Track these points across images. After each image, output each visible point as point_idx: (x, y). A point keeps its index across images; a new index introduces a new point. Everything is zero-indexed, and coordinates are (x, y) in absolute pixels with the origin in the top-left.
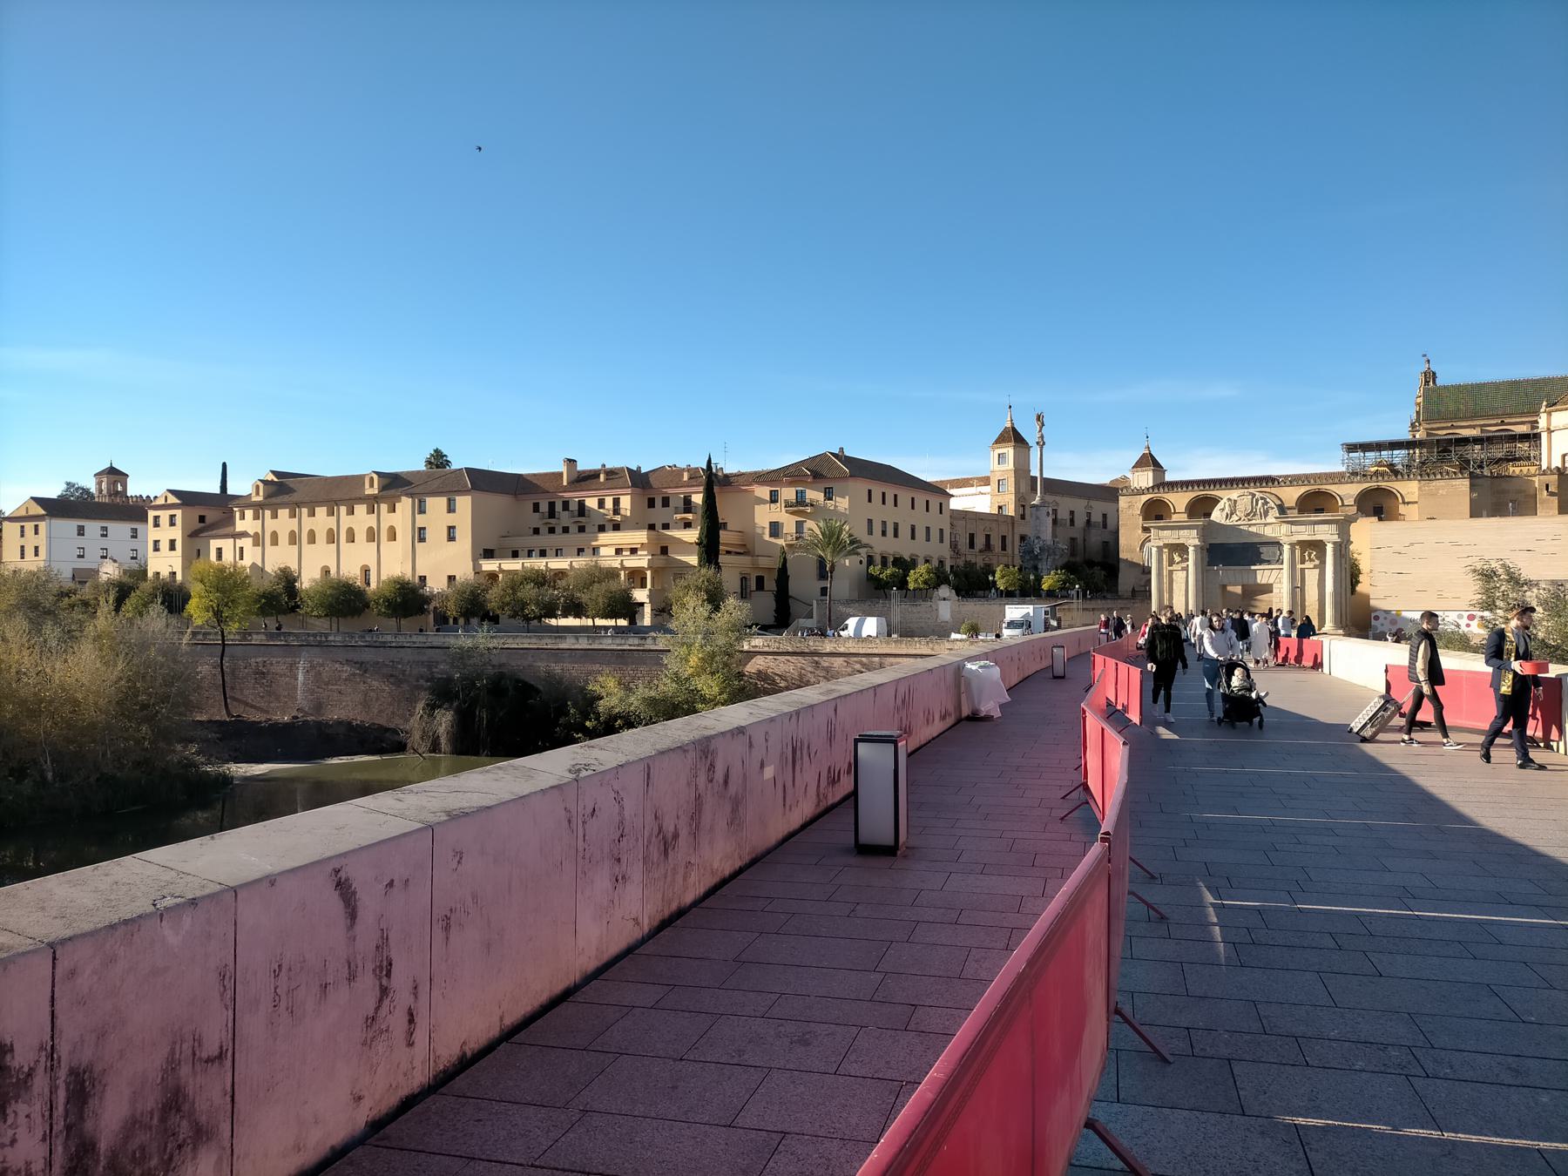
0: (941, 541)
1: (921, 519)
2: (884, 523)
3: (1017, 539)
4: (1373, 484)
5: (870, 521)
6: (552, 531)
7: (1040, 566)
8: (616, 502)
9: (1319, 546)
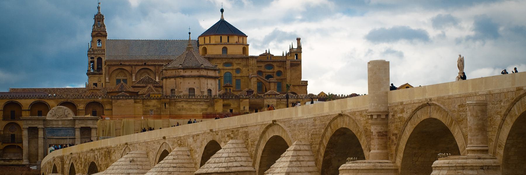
4: (92, 100)
9: (89, 129)
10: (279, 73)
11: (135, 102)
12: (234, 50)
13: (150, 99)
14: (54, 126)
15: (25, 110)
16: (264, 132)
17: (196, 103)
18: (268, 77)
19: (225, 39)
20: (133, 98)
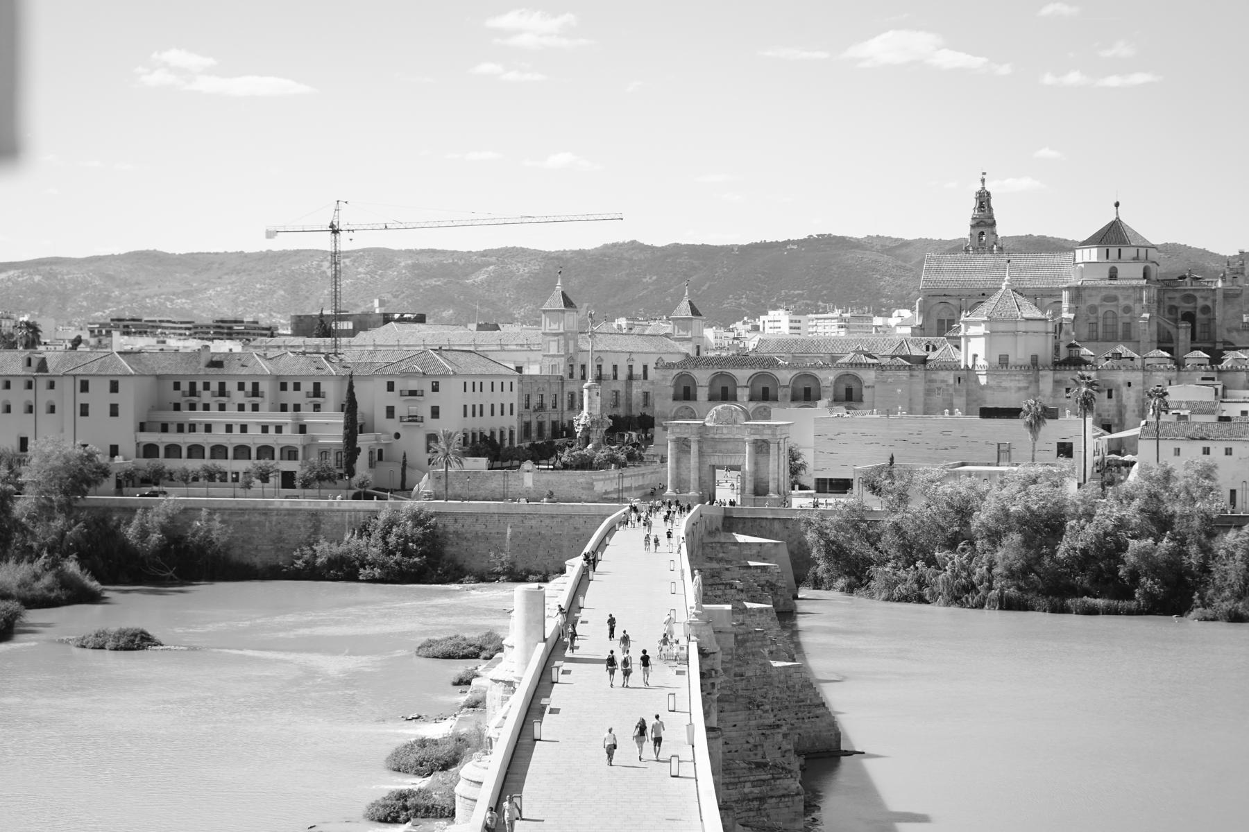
0: (512, 414)
1: (499, 398)
2: (474, 406)
3: (566, 396)
5: (465, 406)
6: (193, 407)
7: (591, 436)
8: (255, 386)
11: (911, 376)
13: (937, 369)
14: (716, 437)
15: (741, 387)
17: (1009, 378)
18: (1189, 317)
20: (907, 368)
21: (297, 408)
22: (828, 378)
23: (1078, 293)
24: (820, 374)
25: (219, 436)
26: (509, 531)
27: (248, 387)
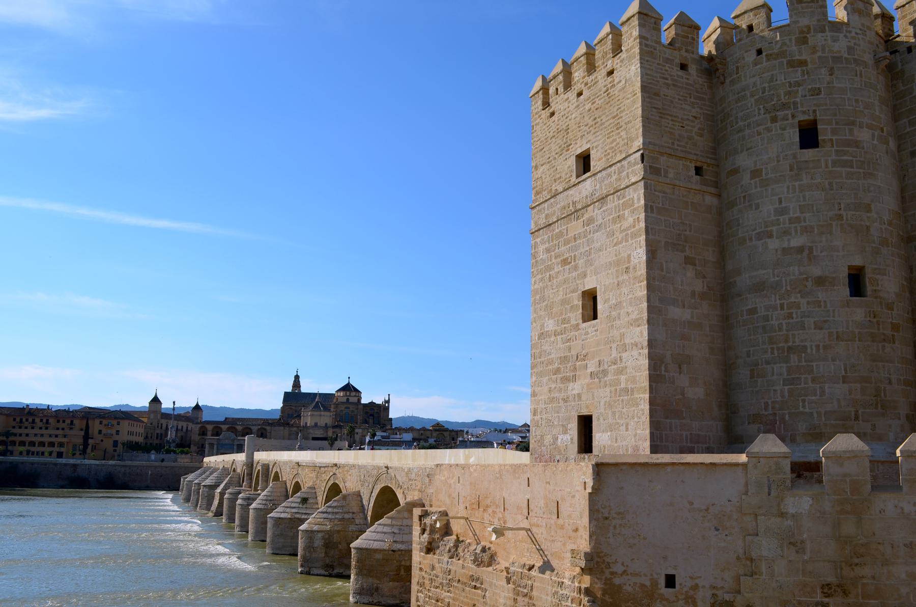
6: (20, 427)
8: (47, 421)
10: (377, 412)
12: (353, 400)
16: (232, 465)
19: (348, 393)
21: (63, 429)
22: (255, 429)
23: (337, 405)
24: (252, 428)
25: (32, 438)
26: (150, 472)
27: (44, 421)
